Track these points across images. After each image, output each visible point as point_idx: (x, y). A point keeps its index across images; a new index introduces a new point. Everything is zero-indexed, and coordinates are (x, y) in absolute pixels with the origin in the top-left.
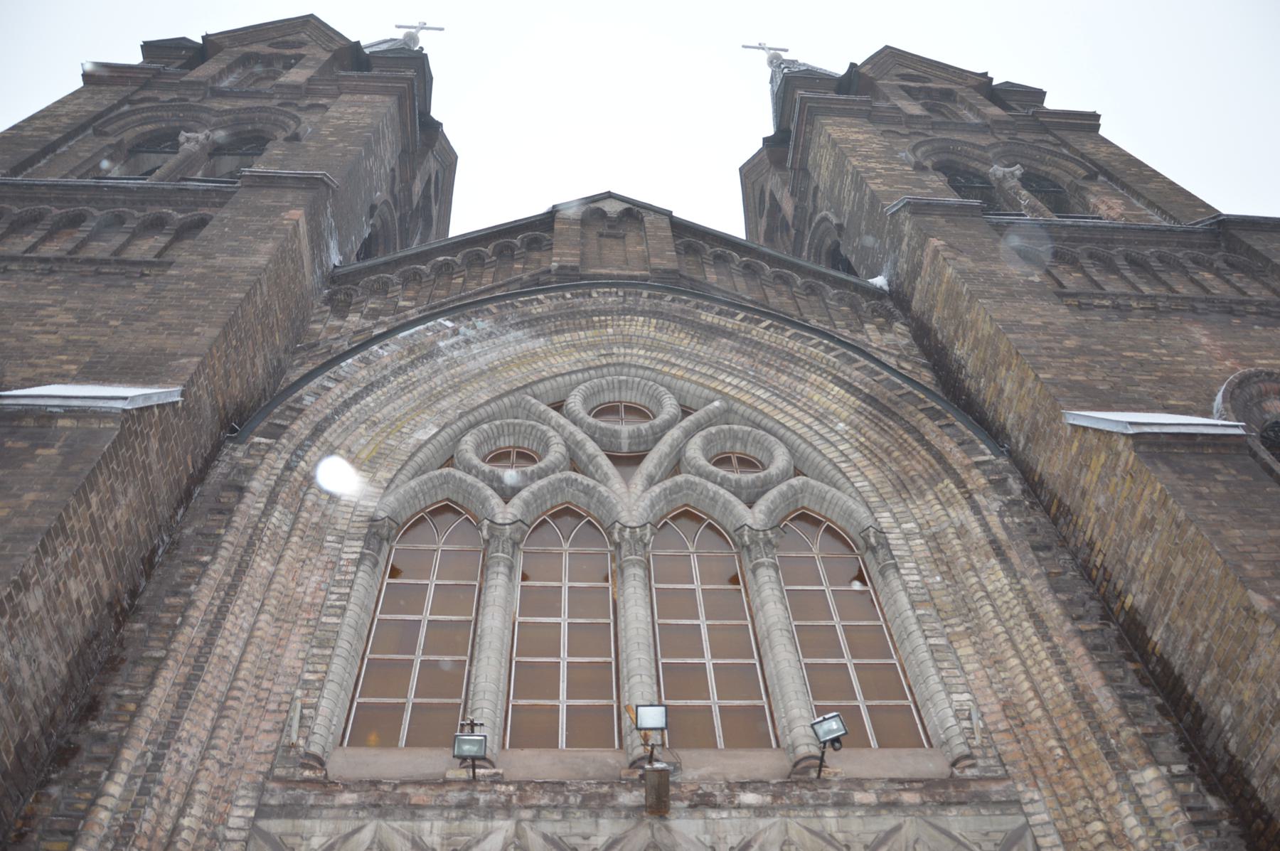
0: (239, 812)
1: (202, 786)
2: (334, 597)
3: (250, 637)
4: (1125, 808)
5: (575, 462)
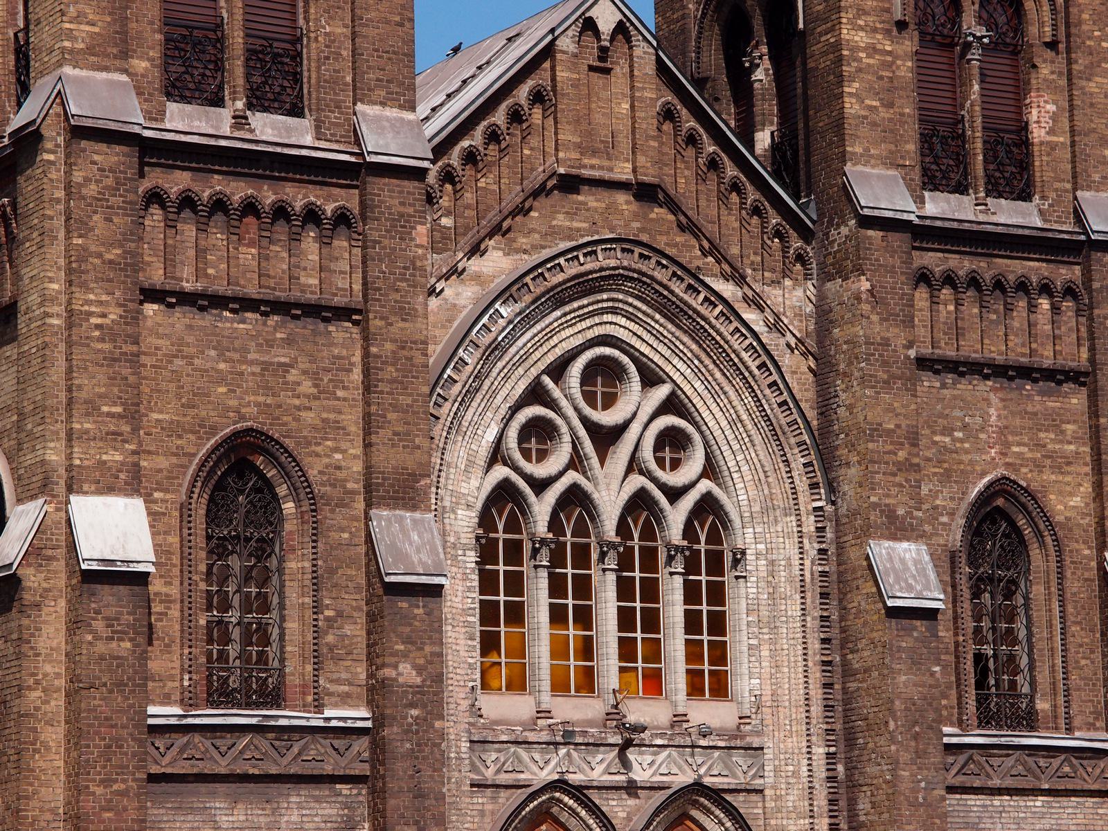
0: (463, 744)
2: (470, 600)
5: (576, 462)
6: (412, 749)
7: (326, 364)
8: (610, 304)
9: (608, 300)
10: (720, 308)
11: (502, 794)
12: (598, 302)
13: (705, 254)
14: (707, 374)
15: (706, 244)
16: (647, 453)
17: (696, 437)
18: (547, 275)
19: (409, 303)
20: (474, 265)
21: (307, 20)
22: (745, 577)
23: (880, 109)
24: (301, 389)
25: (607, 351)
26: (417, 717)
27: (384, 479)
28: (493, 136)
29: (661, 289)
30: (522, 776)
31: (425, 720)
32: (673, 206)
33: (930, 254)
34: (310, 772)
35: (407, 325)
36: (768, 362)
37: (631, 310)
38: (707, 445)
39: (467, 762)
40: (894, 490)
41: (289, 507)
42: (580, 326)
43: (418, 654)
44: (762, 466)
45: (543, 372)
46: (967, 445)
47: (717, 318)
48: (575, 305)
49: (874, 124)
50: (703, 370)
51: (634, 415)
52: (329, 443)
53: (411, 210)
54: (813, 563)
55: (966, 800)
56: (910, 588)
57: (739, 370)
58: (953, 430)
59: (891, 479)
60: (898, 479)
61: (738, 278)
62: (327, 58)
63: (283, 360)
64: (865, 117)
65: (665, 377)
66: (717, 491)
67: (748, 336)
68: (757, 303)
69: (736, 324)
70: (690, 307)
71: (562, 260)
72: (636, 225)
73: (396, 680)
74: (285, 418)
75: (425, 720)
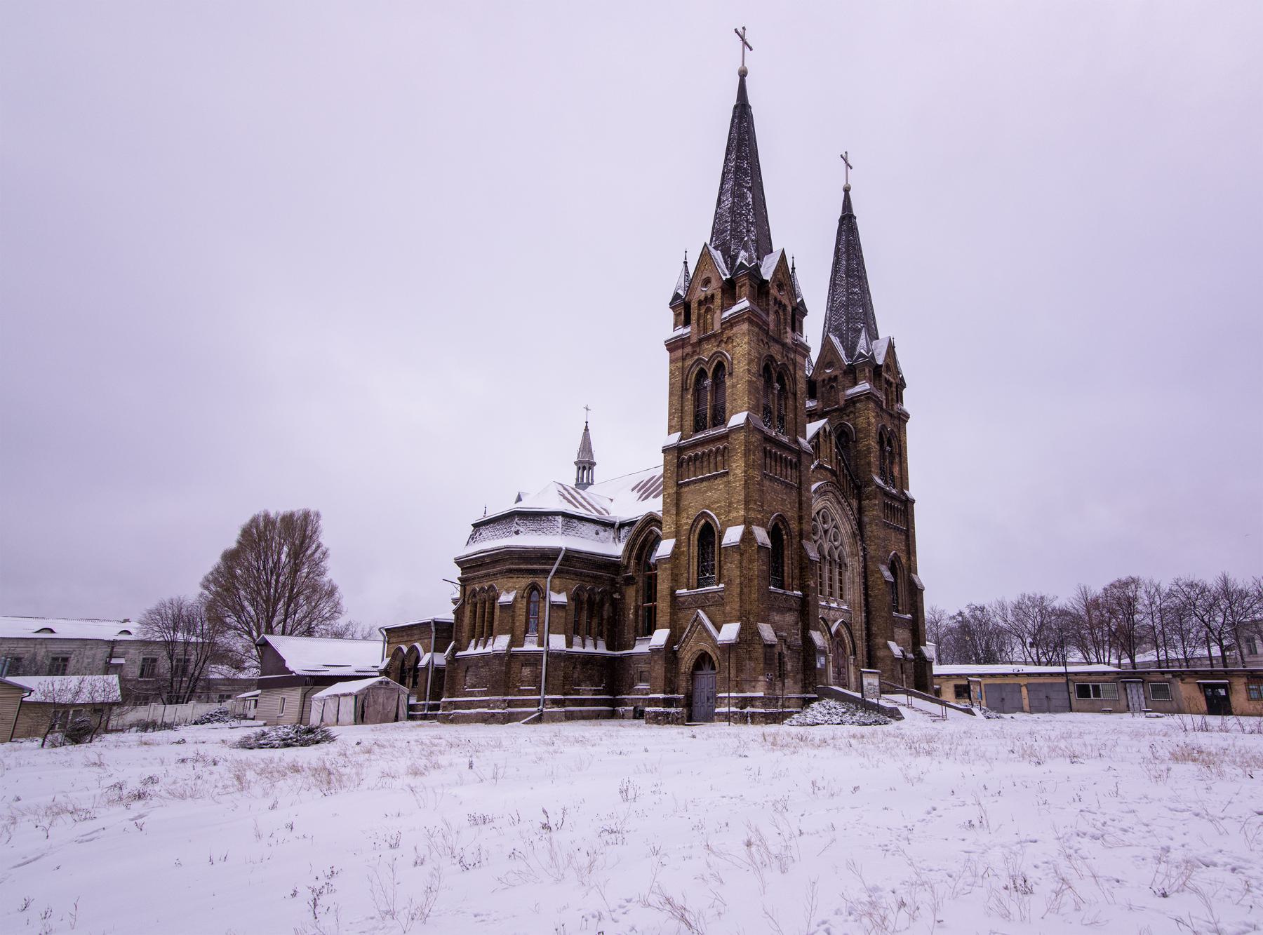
16: (832, 537)
21: (786, 412)
41: (785, 537)
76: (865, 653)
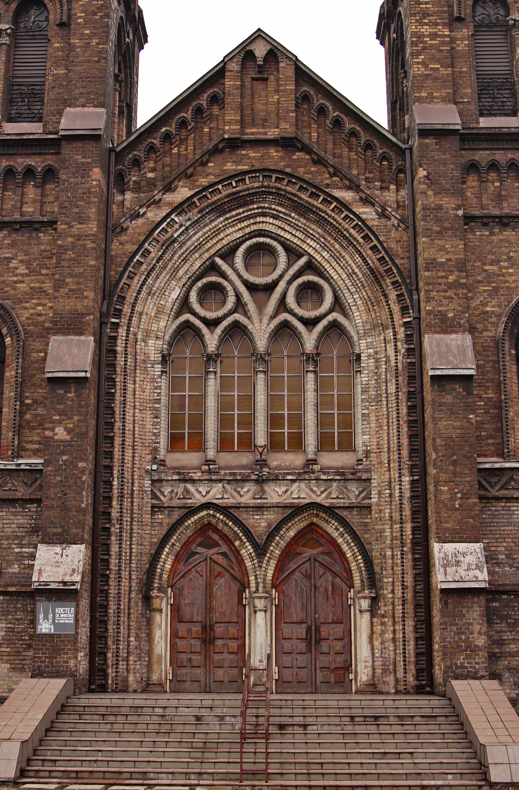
0: (147, 482)
1: (136, 477)
2: (156, 395)
3: (134, 420)
4: (397, 487)
6: (62, 481)
7: (37, 256)
8: (260, 210)
9: (258, 208)
10: (335, 204)
11: (176, 513)
12: (251, 210)
13: (332, 176)
14: (330, 247)
15: (331, 170)
17: (326, 287)
18: (209, 196)
19: (85, 213)
20: (168, 197)
22: (360, 371)
23: (441, 69)
24: (18, 271)
25: (261, 240)
26: (66, 461)
27: (61, 318)
28: (183, 124)
29: (293, 198)
30: (190, 501)
31: (72, 462)
32: (306, 149)
33: (481, 152)
34: (7, 497)
35: (83, 226)
36: (370, 234)
37: (275, 212)
38: (334, 292)
39: (149, 493)
40: (445, 302)
41: (8, 340)
42: (239, 226)
43: (69, 421)
44: (370, 300)
45: (214, 255)
46: (511, 271)
47: (332, 210)
48: (234, 213)
49: (437, 78)
50: (328, 244)
51: (281, 277)
52: (34, 301)
53: (90, 160)
54: (404, 355)
55: (510, 507)
56: (448, 362)
57: (350, 242)
58: (500, 261)
59: (444, 294)
60: (448, 294)
61: (354, 186)
62: (54, 87)
63: (7, 255)
64: (430, 75)
65: (303, 252)
66: (341, 319)
67: (355, 219)
68: (367, 201)
69: (346, 213)
70: (313, 205)
71: (220, 187)
72: (282, 164)
73: (52, 438)
74: (6, 289)
75: (72, 462)
76: (409, 580)
